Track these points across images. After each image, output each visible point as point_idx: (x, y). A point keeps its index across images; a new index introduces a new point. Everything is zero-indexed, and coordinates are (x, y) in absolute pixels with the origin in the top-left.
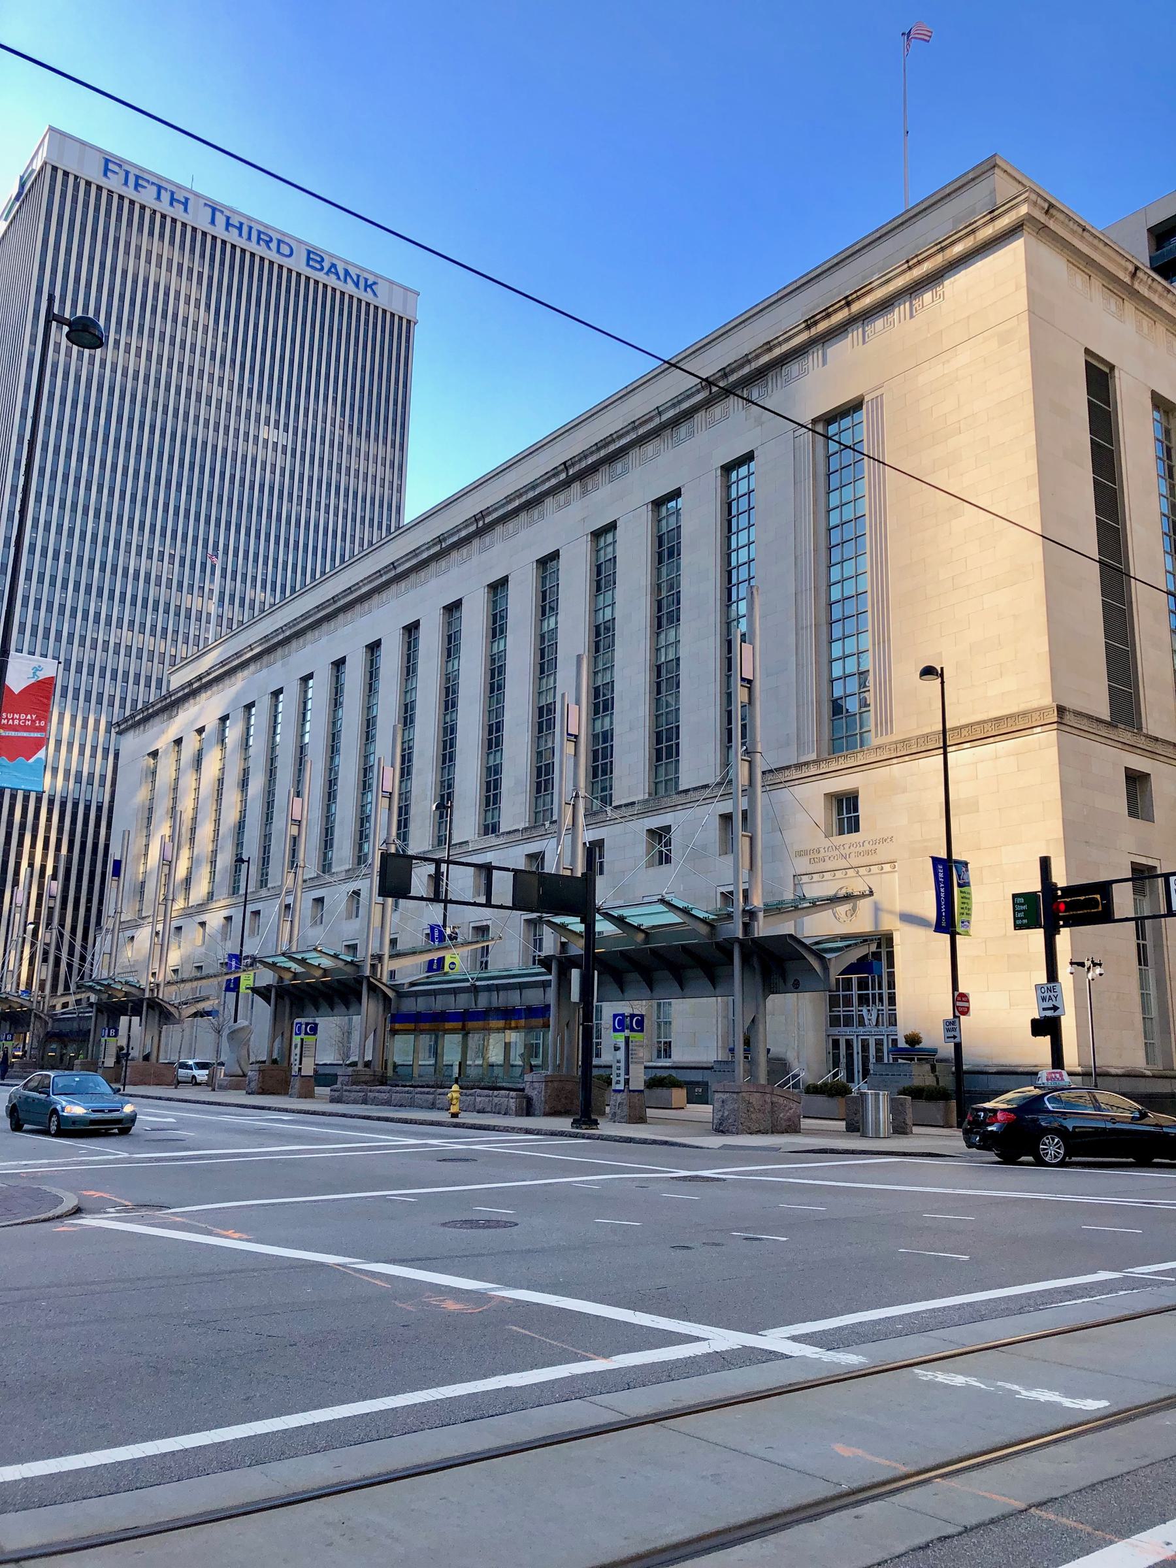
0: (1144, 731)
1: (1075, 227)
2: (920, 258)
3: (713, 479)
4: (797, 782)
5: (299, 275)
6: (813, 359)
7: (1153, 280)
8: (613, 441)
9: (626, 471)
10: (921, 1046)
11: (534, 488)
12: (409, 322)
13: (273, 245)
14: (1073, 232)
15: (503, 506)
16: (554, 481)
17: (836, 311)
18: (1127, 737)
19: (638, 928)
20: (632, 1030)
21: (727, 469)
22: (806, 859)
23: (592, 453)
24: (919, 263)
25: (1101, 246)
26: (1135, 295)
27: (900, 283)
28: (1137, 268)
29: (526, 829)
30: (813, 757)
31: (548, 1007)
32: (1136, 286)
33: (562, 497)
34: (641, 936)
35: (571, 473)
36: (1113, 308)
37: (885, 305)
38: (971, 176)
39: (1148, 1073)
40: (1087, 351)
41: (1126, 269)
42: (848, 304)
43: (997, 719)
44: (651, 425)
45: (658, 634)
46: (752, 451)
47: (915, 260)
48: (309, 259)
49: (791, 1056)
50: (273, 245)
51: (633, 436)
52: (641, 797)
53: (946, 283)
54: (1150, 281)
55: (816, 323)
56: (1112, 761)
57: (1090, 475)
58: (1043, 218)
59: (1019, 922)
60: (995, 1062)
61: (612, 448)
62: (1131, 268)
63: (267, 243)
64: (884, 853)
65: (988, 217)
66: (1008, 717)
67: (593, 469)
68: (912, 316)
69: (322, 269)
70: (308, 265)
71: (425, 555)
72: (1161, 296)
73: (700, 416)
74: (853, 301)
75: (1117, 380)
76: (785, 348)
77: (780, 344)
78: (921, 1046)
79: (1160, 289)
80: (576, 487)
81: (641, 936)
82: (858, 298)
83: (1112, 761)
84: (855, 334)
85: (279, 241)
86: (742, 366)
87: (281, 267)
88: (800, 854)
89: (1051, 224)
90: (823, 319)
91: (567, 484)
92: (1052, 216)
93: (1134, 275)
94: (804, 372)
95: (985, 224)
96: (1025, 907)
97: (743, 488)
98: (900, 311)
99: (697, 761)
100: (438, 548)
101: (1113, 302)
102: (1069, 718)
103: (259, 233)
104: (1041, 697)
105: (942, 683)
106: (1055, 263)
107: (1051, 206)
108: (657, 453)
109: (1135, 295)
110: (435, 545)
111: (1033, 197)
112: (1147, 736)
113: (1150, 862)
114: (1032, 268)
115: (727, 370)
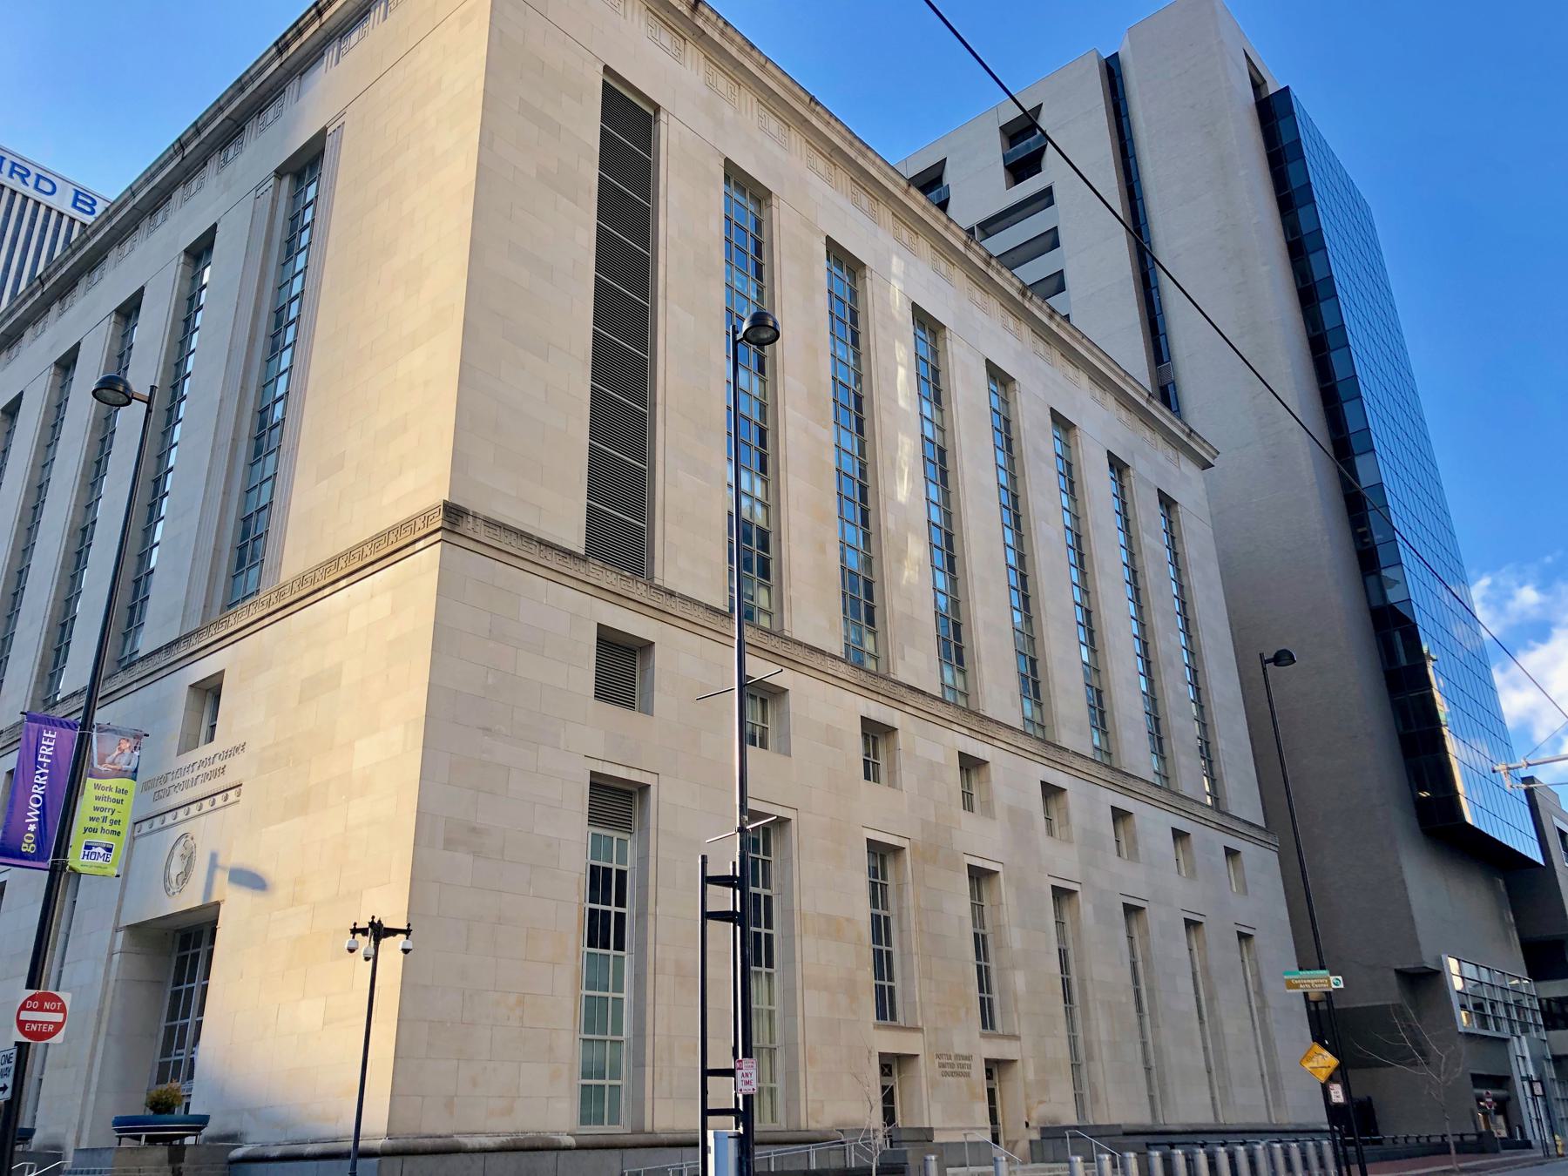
0: (657, 581)
5: (61, 215)
13: (31, 180)
17: (307, 25)
18: (609, 579)
32: (699, 22)
39: (571, 1141)
40: (607, 69)
42: (320, 13)
43: (378, 536)
48: (76, 199)
50: (31, 180)
54: (721, 24)
55: (287, 46)
56: (573, 614)
63: (23, 178)
68: (385, 17)
69: (93, 212)
70: (74, 205)
72: (741, 50)
75: (663, 127)
77: (252, 80)
80: (55, 308)
83: (573, 614)
85: (39, 177)
87: (37, 204)
90: (295, 38)
102: (467, 526)
103: (14, 164)
113: (635, 776)
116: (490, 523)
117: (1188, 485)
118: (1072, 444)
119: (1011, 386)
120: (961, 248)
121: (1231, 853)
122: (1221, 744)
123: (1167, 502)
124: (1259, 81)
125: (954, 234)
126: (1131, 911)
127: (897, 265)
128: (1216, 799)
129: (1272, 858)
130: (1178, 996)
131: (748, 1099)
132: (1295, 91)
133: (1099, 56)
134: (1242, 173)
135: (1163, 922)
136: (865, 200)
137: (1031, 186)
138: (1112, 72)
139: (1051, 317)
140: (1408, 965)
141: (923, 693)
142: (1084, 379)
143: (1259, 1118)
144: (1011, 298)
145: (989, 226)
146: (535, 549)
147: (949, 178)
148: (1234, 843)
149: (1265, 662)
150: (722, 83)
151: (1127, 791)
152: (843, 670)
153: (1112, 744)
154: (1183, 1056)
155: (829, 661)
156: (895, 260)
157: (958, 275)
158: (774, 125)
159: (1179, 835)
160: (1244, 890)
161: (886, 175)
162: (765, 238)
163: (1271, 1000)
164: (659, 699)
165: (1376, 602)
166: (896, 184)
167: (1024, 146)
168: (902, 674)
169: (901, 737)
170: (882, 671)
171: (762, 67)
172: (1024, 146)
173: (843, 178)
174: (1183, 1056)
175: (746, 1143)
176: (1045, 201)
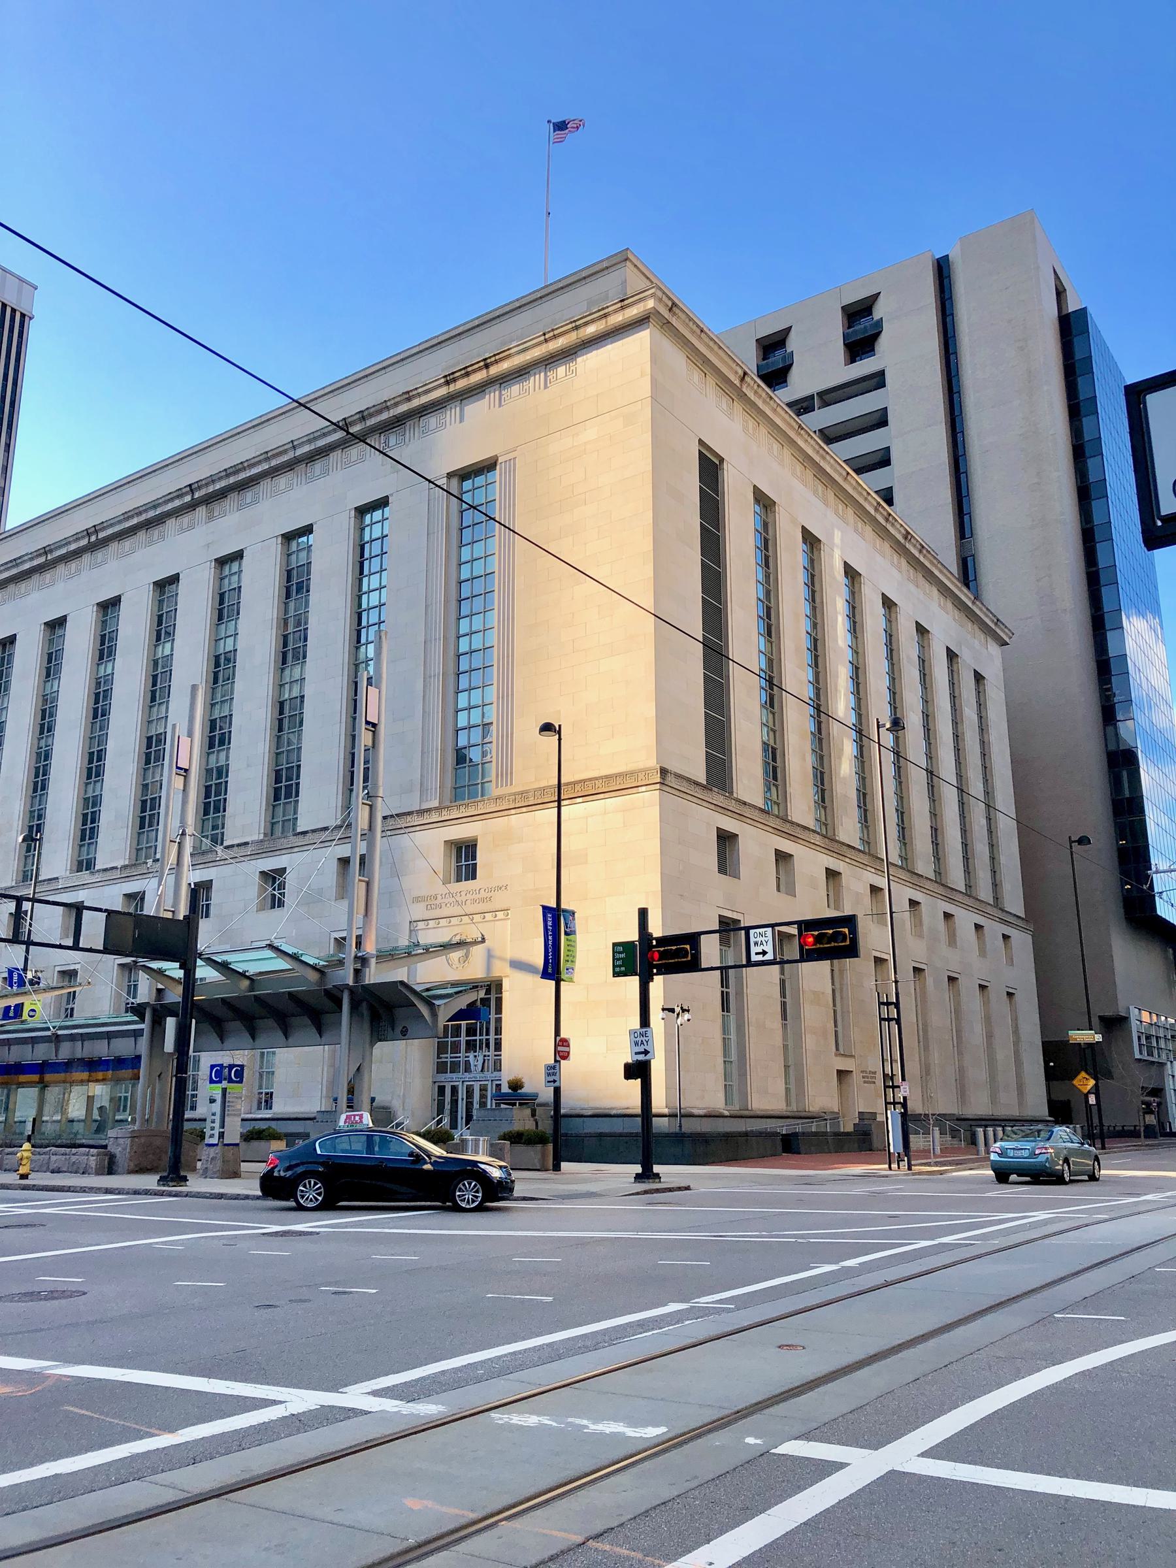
1: (694, 327)
2: (556, 332)
3: (347, 520)
4: (418, 828)
6: (451, 413)
7: (759, 386)
8: (244, 469)
9: (255, 501)
10: (523, 1090)
11: (155, 507)
12: (23, 316)
14: (693, 332)
15: (120, 522)
16: (177, 503)
17: (474, 371)
18: (719, 799)
19: (243, 975)
20: (230, 1081)
21: (362, 511)
22: (422, 905)
23: (220, 479)
24: (555, 337)
25: (716, 348)
26: (743, 397)
27: (536, 353)
28: (745, 374)
29: (125, 867)
30: (435, 803)
31: (139, 1058)
33: (185, 520)
34: (246, 983)
35: (197, 495)
36: (724, 406)
37: (522, 373)
38: (605, 264)
39: (726, 1113)
40: (701, 442)
41: (736, 373)
42: (487, 366)
43: (607, 777)
44: (285, 458)
45: (283, 670)
46: (387, 497)
47: (551, 334)
49: (396, 1105)
51: (265, 466)
52: (255, 838)
53: (579, 360)
55: (454, 380)
56: (706, 821)
57: (698, 557)
58: (666, 314)
59: (617, 969)
60: (592, 1104)
61: (242, 476)
62: (741, 372)
64: (499, 900)
65: (619, 305)
66: (617, 776)
67: (222, 494)
71: (27, 566)
72: (764, 401)
73: (335, 456)
74: (492, 364)
76: (424, 399)
77: (419, 395)
78: (523, 1090)
79: (764, 395)
80: (201, 511)
81: (246, 983)
82: (496, 362)
83: (706, 821)
84: (492, 396)
86: (380, 412)
88: (417, 900)
89: (674, 321)
90: (463, 376)
91: (192, 506)
92: (675, 314)
93: (742, 379)
94: (441, 426)
95: (616, 311)
96: (623, 956)
97: (377, 533)
98: (536, 380)
99: (317, 802)
100: (42, 560)
101: (725, 402)
102: (670, 780)
104: (648, 760)
105: (560, 739)
106: (677, 359)
107: (674, 304)
108: (290, 487)
109: (743, 397)
110: (40, 555)
111: (659, 294)
112: (738, 800)
113: (735, 916)
114: (655, 358)
115: (366, 413)
116: (679, 776)
117: (986, 657)
118: (926, 645)
119: (893, 609)
120: (872, 512)
121: (1006, 937)
122: (1003, 859)
123: (979, 678)
124: (1061, 289)
125: (870, 503)
126: (952, 979)
127: (837, 536)
128: (996, 899)
129: (1029, 939)
130: (976, 1034)
131: (905, 1098)
132: (1090, 310)
133: (933, 256)
134: (1045, 388)
135: (968, 986)
136: (820, 488)
137: (865, 367)
138: (943, 270)
139: (920, 552)
140: (1108, 1013)
141: (854, 848)
142: (935, 592)
143: (1015, 1112)
144: (898, 542)
145: (830, 397)
146: (685, 783)
147: (793, 344)
148: (1008, 931)
149: (1071, 842)
150: (751, 423)
151: (951, 900)
152: (817, 839)
153: (942, 867)
154: (978, 1074)
155: (812, 835)
156: (836, 531)
157: (868, 530)
158: (776, 446)
159: (978, 927)
160: (1010, 961)
161: (836, 470)
162: (770, 537)
163: (1023, 1038)
164: (744, 870)
165: (1112, 747)
166: (841, 474)
167: (861, 331)
168: (842, 836)
169: (844, 879)
170: (830, 834)
171: (774, 411)
172: (861, 331)
173: (809, 474)
174: (978, 1074)
175: (904, 1115)
176: (874, 382)
